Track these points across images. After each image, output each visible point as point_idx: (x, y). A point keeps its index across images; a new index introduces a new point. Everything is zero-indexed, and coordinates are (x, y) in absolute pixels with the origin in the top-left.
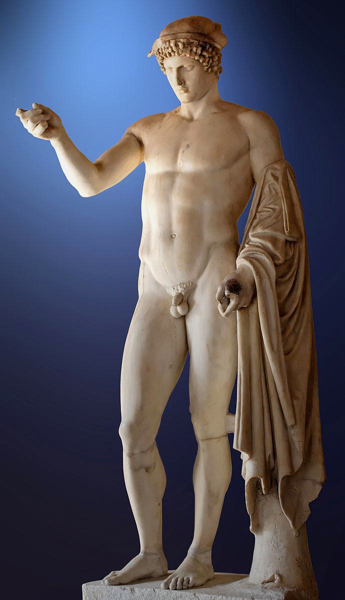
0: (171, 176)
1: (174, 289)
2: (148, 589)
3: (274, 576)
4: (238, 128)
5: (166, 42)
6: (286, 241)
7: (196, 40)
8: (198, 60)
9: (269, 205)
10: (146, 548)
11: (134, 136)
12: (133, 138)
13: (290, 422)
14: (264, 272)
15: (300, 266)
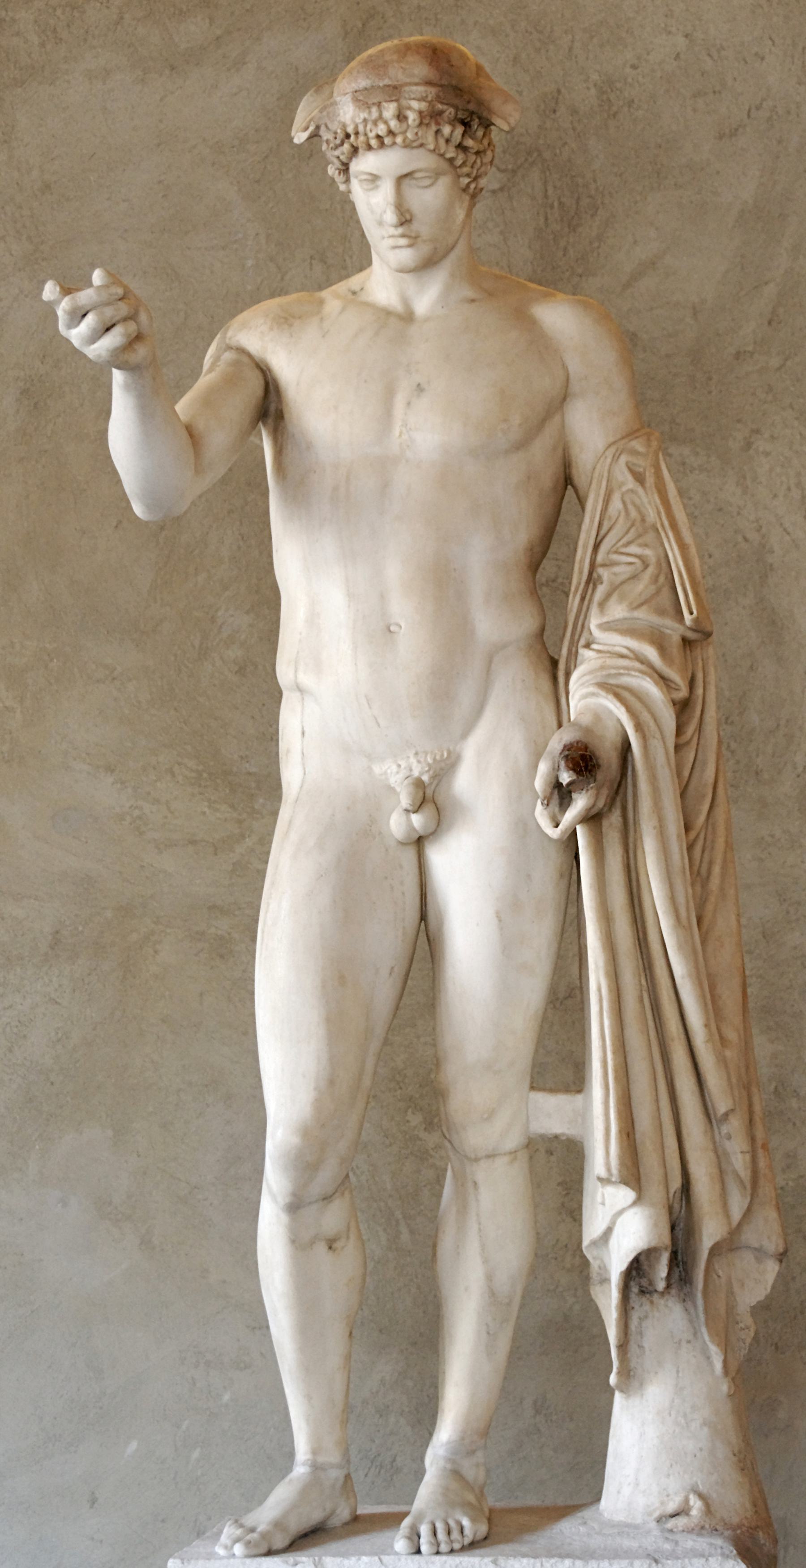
1: (399, 766)
3: (687, 1500)
4: (540, 344)
5: (369, 108)
7: (452, 106)
8: (451, 161)
9: (629, 543)
10: (315, 1452)
11: (249, 355)
12: (246, 360)
13: (722, 1105)
14: (652, 723)
15: (707, 706)
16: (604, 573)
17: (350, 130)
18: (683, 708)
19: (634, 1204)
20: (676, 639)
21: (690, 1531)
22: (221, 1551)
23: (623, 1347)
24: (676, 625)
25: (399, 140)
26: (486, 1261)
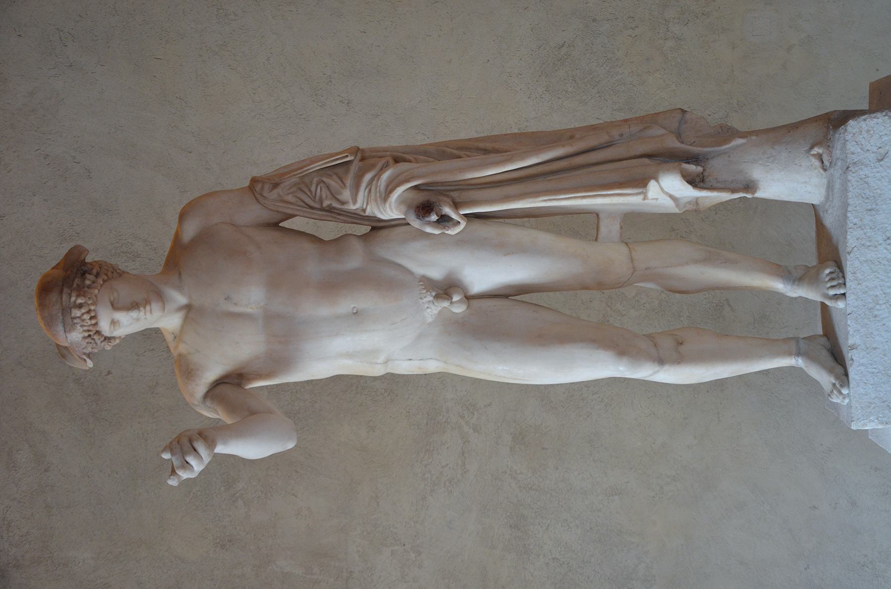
2: (849, 322)
3: (814, 155)
8: (104, 281)
9: (310, 191)
10: (790, 354)
11: (208, 392)
16: (326, 203)
17: (86, 334)
18: (397, 160)
19: (657, 181)
20: (360, 164)
21: (830, 154)
22: (847, 401)
23: (733, 191)
24: (354, 164)
25: (92, 308)
26: (687, 264)
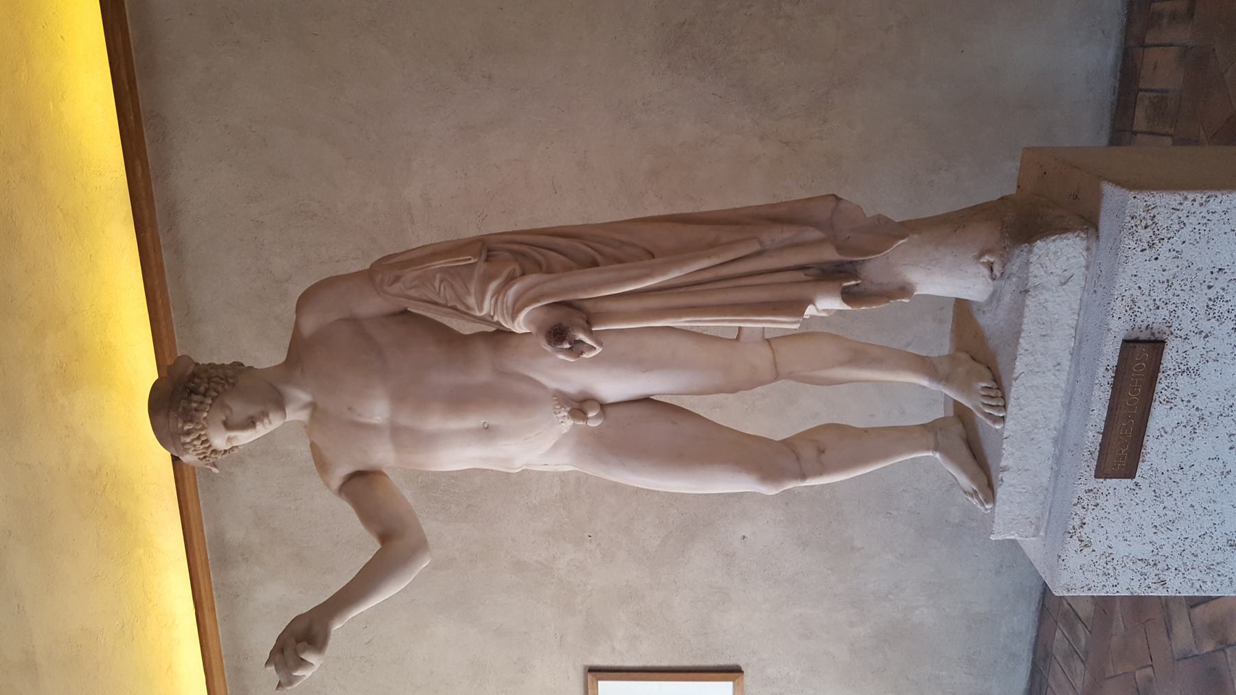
0: (396, 432)
6: (486, 260)
8: (213, 399)
10: (928, 449)
13: (756, 247)
26: (833, 367)
